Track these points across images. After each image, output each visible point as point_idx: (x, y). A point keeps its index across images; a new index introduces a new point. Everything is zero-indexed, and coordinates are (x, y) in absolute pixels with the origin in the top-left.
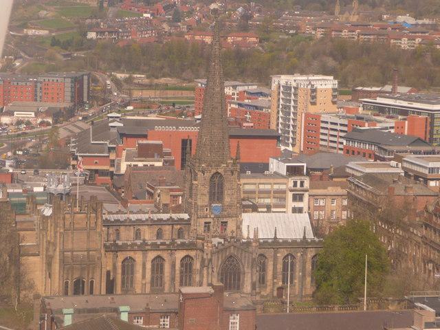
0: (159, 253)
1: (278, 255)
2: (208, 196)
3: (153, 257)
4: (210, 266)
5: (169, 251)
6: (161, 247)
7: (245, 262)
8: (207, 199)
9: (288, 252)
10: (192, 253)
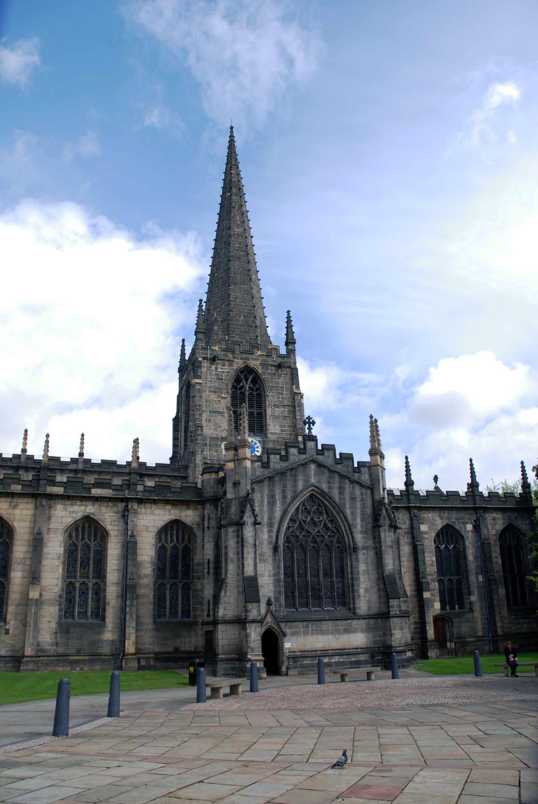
0: (90, 509)
1: (424, 528)
3: (69, 520)
5: (121, 506)
6: (96, 492)
7: (353, 514)
9: (445, 522)
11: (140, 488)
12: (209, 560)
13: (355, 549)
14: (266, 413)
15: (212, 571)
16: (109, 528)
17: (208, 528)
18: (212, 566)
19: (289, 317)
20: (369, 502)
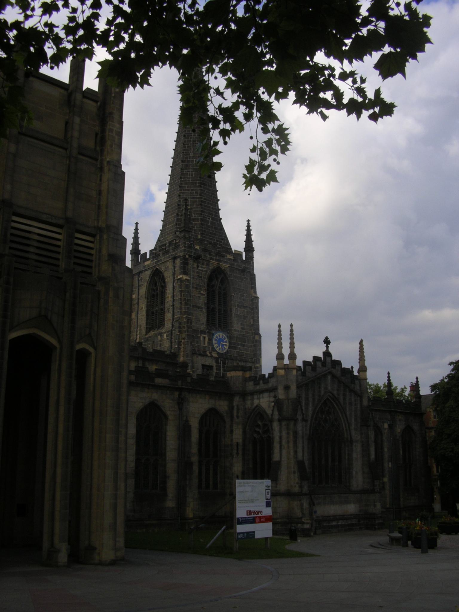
0: (155, 396)
2: (205, 311)
4: (299, 417)
5: (176, 394)
8: (203, 319)
10: (222, 406)
11: (189, 380)
12: (237, 443)
13: (351, 442)
14: (231, 311)
15: (240, 452)
16: (168, 413)
17: (238, 417)
18: (240, 448)
19: (248, 226)
20: (359, 406)
